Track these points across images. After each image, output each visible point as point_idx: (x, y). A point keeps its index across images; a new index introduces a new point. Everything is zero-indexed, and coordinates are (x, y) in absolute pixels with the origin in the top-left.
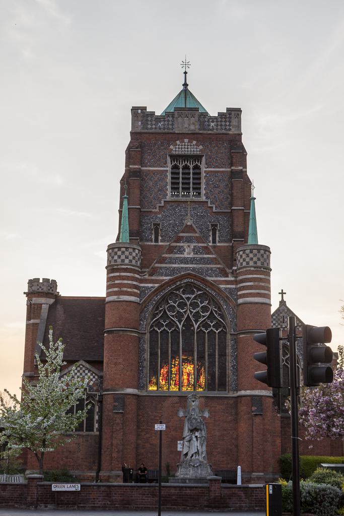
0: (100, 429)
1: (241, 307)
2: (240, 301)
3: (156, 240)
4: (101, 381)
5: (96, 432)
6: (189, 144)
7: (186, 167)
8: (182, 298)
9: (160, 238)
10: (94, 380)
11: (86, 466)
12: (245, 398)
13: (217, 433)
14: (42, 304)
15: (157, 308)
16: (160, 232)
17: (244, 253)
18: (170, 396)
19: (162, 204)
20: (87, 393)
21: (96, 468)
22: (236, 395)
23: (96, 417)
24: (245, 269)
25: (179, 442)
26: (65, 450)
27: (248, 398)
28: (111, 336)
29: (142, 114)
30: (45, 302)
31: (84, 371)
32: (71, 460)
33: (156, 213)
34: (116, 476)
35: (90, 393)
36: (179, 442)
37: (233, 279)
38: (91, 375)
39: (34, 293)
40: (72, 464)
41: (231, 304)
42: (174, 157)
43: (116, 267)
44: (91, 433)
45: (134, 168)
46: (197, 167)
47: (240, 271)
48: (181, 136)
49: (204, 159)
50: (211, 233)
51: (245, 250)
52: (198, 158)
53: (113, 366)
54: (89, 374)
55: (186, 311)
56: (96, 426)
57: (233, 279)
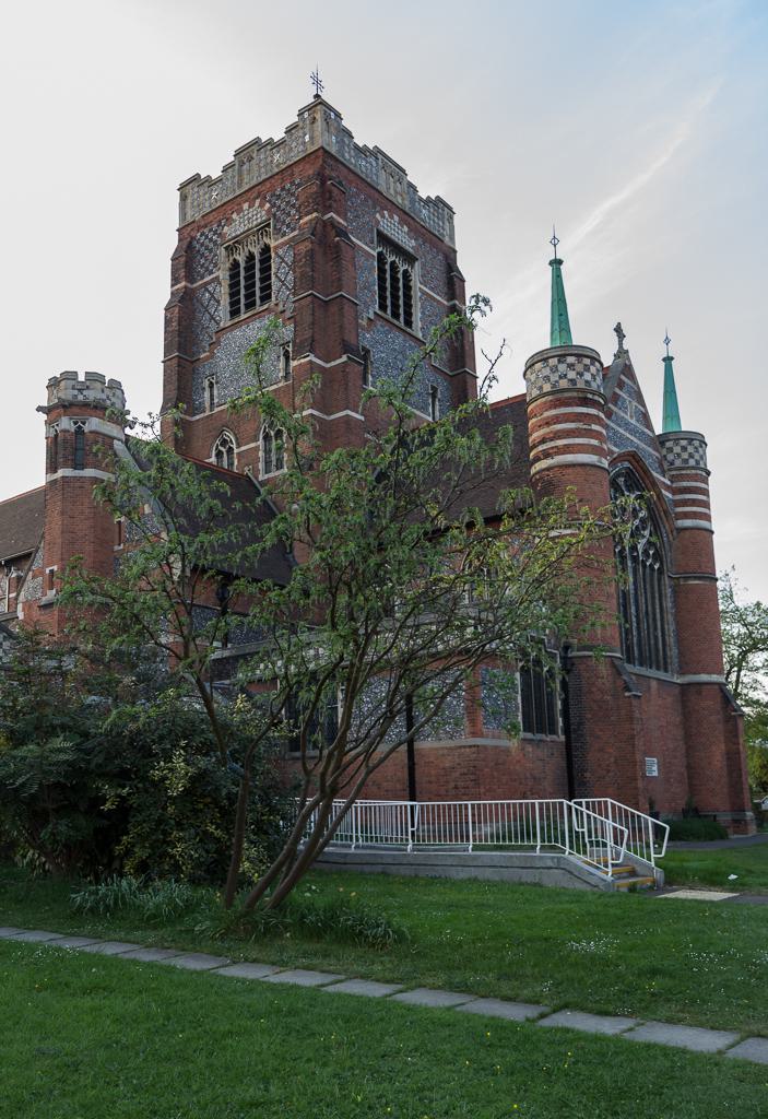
1: (687, 533)
2: (688, 523)
14: (114, 438)
19: (372, 316)
24: (693, 471)
37: (669, 483)
42: (383, 239)
45: (339, 223)
46: (406, 274)
47: (684, 472)
48: (394, 208)
50: (430, 401)
51: (693, 440)
52: (410, 259)
57: (669, 483)
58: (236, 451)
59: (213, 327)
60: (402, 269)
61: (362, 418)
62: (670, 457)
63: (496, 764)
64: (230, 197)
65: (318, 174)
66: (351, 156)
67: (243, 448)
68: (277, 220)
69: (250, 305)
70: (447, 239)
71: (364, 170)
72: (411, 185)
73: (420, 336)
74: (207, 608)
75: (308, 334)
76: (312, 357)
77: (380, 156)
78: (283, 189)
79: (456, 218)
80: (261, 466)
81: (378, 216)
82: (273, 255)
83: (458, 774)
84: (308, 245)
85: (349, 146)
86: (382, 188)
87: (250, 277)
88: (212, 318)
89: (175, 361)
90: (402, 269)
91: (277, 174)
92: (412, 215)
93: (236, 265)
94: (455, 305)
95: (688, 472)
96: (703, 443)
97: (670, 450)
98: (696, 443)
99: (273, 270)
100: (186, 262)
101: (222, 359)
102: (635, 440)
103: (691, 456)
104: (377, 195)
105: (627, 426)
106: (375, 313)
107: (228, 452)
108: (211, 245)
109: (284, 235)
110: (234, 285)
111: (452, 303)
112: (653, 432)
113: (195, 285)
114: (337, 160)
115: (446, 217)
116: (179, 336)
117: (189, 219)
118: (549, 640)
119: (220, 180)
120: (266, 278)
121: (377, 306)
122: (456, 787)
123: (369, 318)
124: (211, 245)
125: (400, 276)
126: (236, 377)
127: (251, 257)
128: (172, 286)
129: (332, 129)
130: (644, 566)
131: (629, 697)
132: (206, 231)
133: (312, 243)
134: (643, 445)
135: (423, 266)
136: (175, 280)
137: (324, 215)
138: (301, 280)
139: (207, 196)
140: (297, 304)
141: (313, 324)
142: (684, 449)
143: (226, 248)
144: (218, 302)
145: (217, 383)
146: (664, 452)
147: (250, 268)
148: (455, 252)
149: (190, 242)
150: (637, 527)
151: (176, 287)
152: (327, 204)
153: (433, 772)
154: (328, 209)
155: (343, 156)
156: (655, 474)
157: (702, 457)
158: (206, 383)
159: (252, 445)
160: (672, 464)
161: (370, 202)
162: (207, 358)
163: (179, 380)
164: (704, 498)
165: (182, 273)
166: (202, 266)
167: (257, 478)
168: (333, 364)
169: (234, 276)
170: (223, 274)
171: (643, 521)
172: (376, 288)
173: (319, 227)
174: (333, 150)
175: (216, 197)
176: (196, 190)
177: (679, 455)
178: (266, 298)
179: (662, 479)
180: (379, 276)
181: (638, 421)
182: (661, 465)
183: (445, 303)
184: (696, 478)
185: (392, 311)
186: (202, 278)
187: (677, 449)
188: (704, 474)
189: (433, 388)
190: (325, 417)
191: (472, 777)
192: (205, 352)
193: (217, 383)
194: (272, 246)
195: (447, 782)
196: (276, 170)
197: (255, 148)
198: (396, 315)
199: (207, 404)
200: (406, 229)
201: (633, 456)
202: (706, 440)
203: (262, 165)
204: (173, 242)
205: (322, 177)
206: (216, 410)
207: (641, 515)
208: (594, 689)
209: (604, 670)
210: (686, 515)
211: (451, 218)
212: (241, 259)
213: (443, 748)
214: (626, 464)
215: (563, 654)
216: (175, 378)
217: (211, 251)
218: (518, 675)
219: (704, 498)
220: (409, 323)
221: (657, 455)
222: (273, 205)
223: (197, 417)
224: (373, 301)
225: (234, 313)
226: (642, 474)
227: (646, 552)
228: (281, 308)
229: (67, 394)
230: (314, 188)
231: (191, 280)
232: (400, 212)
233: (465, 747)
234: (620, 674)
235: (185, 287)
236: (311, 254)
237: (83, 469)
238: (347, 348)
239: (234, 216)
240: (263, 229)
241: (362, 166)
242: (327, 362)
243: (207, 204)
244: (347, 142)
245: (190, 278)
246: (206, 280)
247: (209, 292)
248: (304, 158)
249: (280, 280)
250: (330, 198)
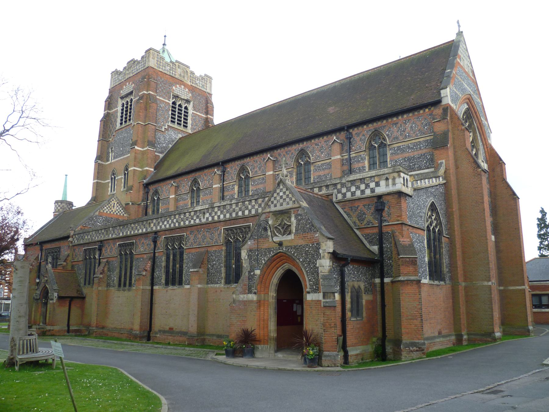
6: (184, 90)
19: (166, 127)
46: (186, 108)
49: (191, 103)
58: (116, 178)
60: (184, 106)
69: (126, 122)
79: (213, 81)
81: (174, 88)
90: (184, 106)
148: (211, 95)
170: (119, 108)
183: (204, 116)
204: (106, 94)
220: (185, 127)
235: (107, 112)
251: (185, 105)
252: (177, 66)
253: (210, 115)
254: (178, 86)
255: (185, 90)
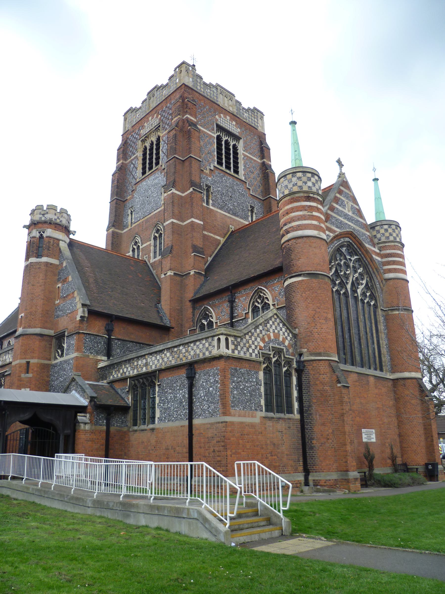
0: (301, 411)
2: (391, 275)
3: (208, 203)
4: (296, 341)
5: (297, 416)
6: (230, 122)
7: (226, 142)
8: (346, 259)
9: (211, 202)
10: (289, 338)
11: (291, 466)
12: (409, 381)
13: (386, 420)
14: (59, 240)
15: (331, 262)
16: (211, 195)
17: (389, 227)
18: (351, 372)
19: (212, 168)
20: (284, 357)
21: (301, 468)
22: (392, 377)
23: (295, 394)
24: (393, 244)
25: (363, 430)
26: (268, 442)
27: (414, 380)
28: (314, 280)
29: (192, 73)
30: (63, 239)
31: (278, 324)
32: (276, 457)
33: (207, 175)
34: (355, 479)
35: (288, 356)
36: (363, 430)
37: (378, 251)
38: (286, 331)
39: (50, 223)
40: (277, 464)
41: (378, 277)
42: (220, 128)
43: (311, 195)
44: (290, 416)
45: (191, 120)
46: (235, 147)
47: (387, 244)
48: (226, 112)
49: (241, 141)
50: (250, 214)
51: (391, 225)
52: (237, 138)
53: (324, 321)
54: (284, 330)
55: (349, 274)
56: (296, 405)
57: (378, 251)
58: (141, 247)
59: (134, 182)
60: (232, 144)
61: (202, 223)
62: (379, 236)
63: (241, 435)
64: (144, 115)
65: (181, 97)
66: (201, 88)
67: (144, 245)
68: (163, 123)
69: (151, 168)
70: (260, 129)
71: (209, 94)
72: (237, 102)
73: (243, 178)
74: (98, 336)
75: (172, 179)
76: (174, 191)
77: (219, 88)
78: (166, 107)
79: (265, 118)
80: (152, 255)
81: (217, 117)
82: (161, 140)
83: (215, 441)
84: (174, 132)
85: (200, 83)
86: (221, 103)
87: (151, 154)
88: (134, 177)
89: (115, 201)
91: (164, 100)
92: (238, 116)
93: (145, 148)
94: (264, 162)
95: (389, 244)
96: (398, 226)
97: (378, 232)
98: (394, 227)
99: (161, 148)
100: (123, 150)
101: (137, 198)
102: (352, 225)
103: (391, 235)
104: (217, 106)
105: (346, 216)
106: (214, 166)
107: (137, 248)
108: (135, 140)
109: (166, 130)
110: (144, 159)
111: (263, 160)
112: (365, 220)
113: (127, 162)
114: (192, 89)
115: (259, 117)
116: (117, 188)
117: (127, 129)
118: (288, 351)
119: (140, 108)
120: (158, 154)
121: (216, 163)
122: (214, 451)
123: (210, 169)
124: (135, 140)
125: (231, 147)
126: (142, 206)
127: (152, 144)
128: (117, 163)
129: (190, 75)
130: (363, 302)
131: (339, 387)
132: (133, 134)
133: (176, 131)
134: (357, 228)
135: (245, 143)
136: (118, 160)
137: (183, 117)
138: (170, 150)
139: (134, 117)
140: (168, 163)
141: (175, 173)
142: (386, 230)
143: (142, 141)
144: (136, 168)
145: (134, 211)
146: (374, 233)
147: (151, 149)
148: (265, 134)
149: (126, 141)
150: (357, 278)
151: (118, 164)
152: (185, 110)
153: (202, 440)
154: (186, 113)
155: (197, 88)
156: (367, 245)
157: (397, 235)
158: (130, 211)
159: (148, 243)
160: (380, 240)
161: (212, 110)
162: (131, 198)
163: (116, 211)
164: (401, 260)
165: (121, 156)
166: (131, 151)
167: (149, 262)
168: (186, 193)
169: (144, 154)
170: (140, 154)
171: (360, 274)
172: (216, 153)
173: (181, 124)
174: (191, 85)
175: (139, 116)
176: (130, 114)
177: (383, 234)
178: (157, 164)
179: (373, 249)
180: (217, 147)
181: (354, 213)
182: (372, 240)
183: (259, 161)
184: (394, 248)
185: (226, 165)
186: (131, 157)
187: (382, 231)
188: (400, 245)
189: (251, 206)
190: (181, 223)
191: (223, 444)
192: (130, 195)
193: (134, 211)
194: (161, 136)
195: (209, 447)
196: (164, 98)
197: (156, 89)
198: (228, 167)
199: (129, 223)
200: (234, 123)
201: (351, 234)
202: (400, 226)
203: (158, 97)
204: (119, 141)
205: (183, 98)
206: (133, 226)
207: (359, 271)
208: (318, 382)
209: (324, 368)
210: (390, 271)
211: (262, 118)
212: (148, 145)
213: (207, 424)
214: (347, 239)
215: (298, 359)
216: (114, 210)
217: (135, 143)
218: (261, 375)
219: (401, 260)
220: (236, 171)
221: (368, 234)
222: (162, 116)
223: (125, 231)
224: (213, 161)
225: (144, 173)
226: (359, 245)
227: (364, 294)
228: (163, 167)
229: (37, 217)
230: (179, 104)
231: (125, 158)
232: (229, 114)
233: (219, 423)
234: (334, 372)
235: (122, 163)
236: (175, 136)
237: (41, 258)
238: (193, 184)
239: (145, 124)
240: (157, 128)
241: (208, 92)
242: (183, 193)
243: (134, 121)
244: (199, 81)
245: (125, 158)
246: (132, 158)
247: (133, 164)
248: (176, 90)
249: (164, 153)
250: (186, 108)
251: (233, 143)
252: (219, 90)
253: (267, 160)
254: (222, 115)
255: (232, 122)
